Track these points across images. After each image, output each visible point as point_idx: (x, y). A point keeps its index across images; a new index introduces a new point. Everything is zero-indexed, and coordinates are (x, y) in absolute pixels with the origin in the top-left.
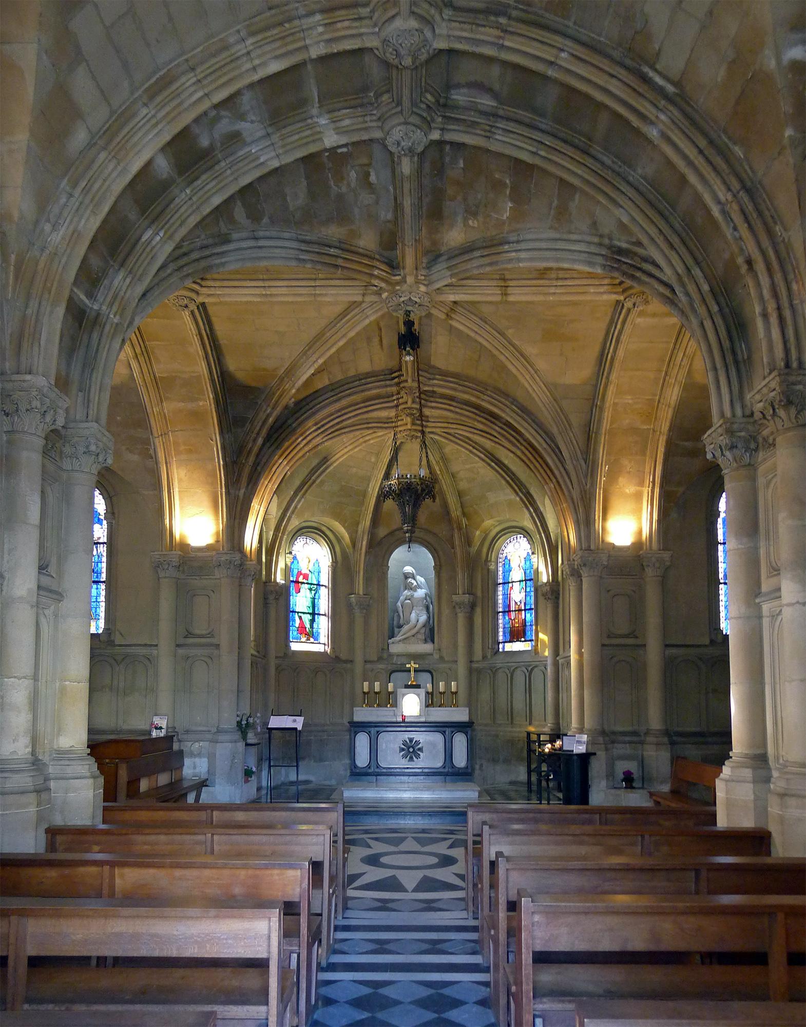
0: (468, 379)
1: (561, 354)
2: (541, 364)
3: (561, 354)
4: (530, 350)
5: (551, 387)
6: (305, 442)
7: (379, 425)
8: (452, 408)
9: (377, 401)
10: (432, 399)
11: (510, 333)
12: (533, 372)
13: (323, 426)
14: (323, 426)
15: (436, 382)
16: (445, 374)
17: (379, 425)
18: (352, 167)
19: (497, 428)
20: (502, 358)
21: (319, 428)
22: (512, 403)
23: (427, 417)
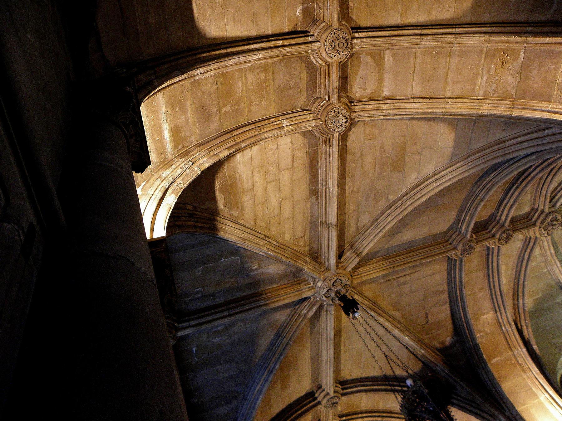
0: (465, 203)
1: (420, 153)
2: (429, 169)
3: (420, 153)
4: (413, 179)
5: (455, 159)
6: (507, 326)
7: (528, 250)
8: (509, 205)
9: (490, 260)
10: (498, 218)
11: (392, 198)
12: (433, 179)
13: (499, 307)
14: (499, 307)
15: (463, 229)
16: (458, 221)
17: (528, 250)
18: (209, 341)
19: (534, 173)
20: (409, 209)
21: (500, 310)
22: (489, 175)
23: (533, 209)
